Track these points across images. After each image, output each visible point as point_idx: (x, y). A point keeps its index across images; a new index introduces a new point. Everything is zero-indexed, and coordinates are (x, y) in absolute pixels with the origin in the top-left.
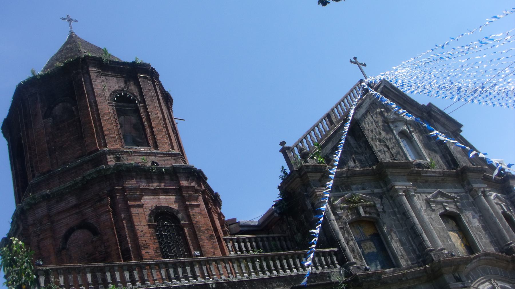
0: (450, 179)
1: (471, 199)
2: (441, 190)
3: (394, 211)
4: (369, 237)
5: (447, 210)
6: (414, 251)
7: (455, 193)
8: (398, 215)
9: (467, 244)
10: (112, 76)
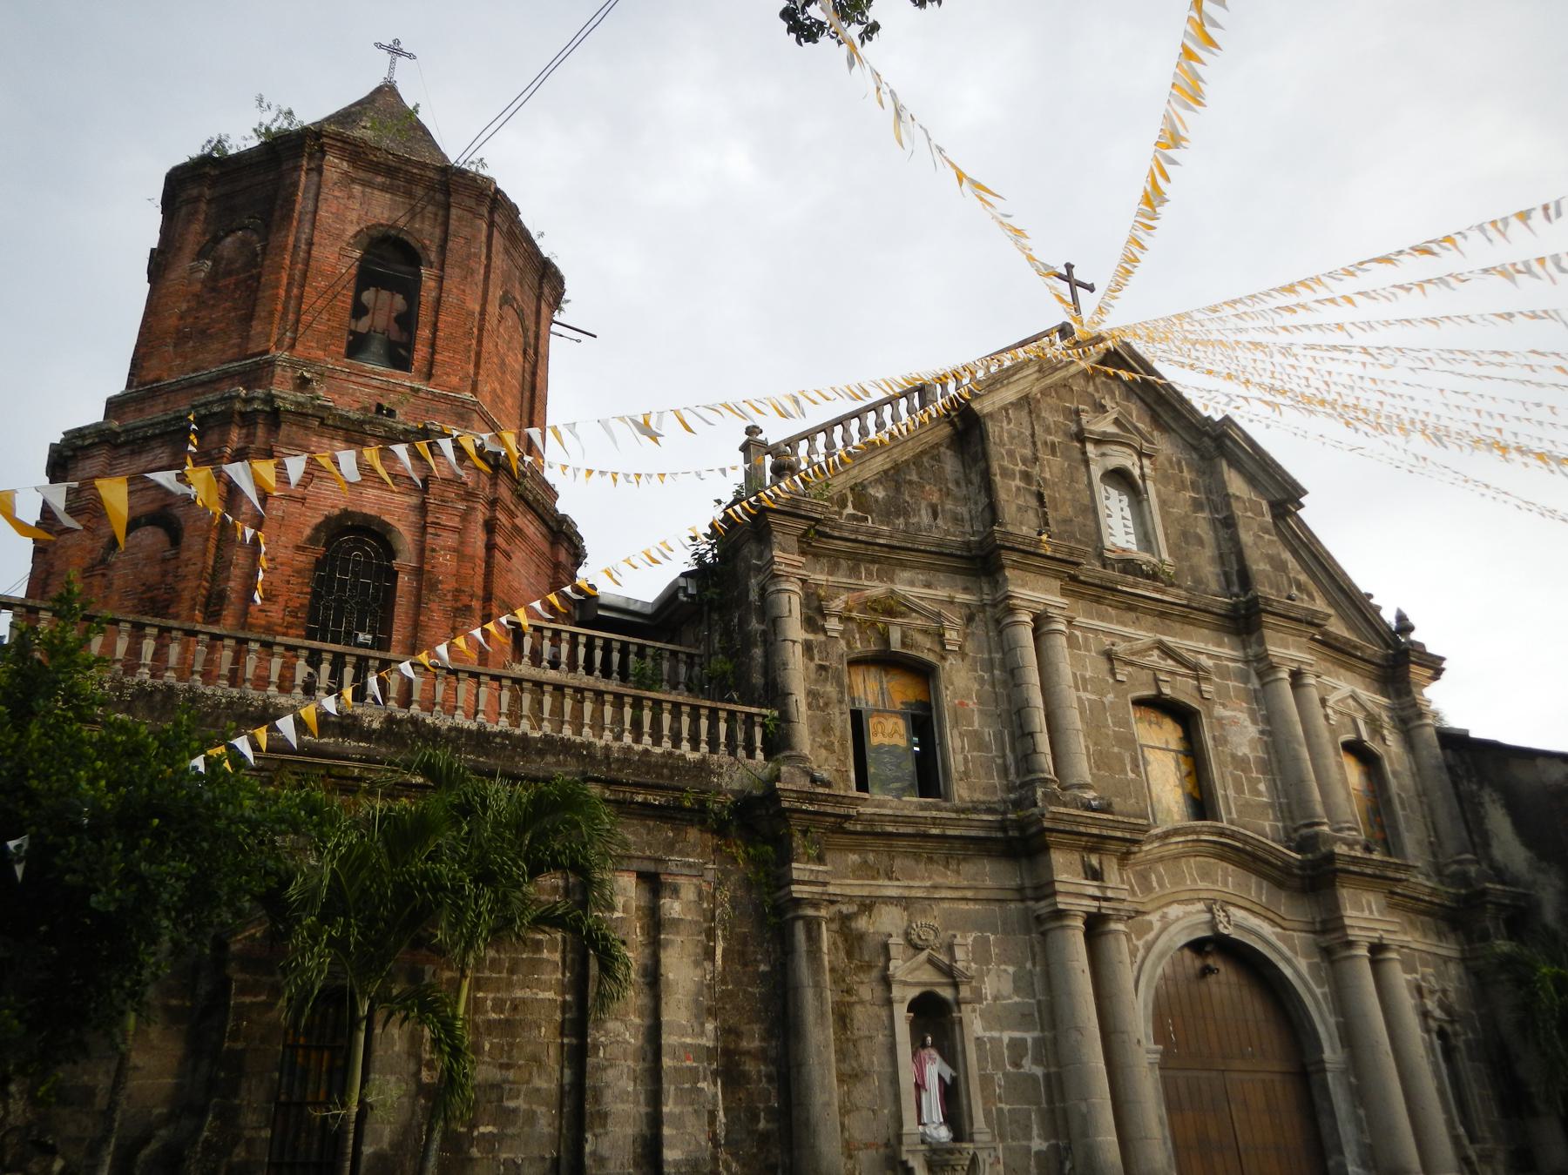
0: (1208, 618)
1: (1255, 683)
2: (1165, 638)
3: (991, 660)
4: (899, 707)
5: (1160, 692)
6: (1004, 771)
7: (1210, 656)
8: (997, 672)
9: (1196, 795)
10: (383, 189)
